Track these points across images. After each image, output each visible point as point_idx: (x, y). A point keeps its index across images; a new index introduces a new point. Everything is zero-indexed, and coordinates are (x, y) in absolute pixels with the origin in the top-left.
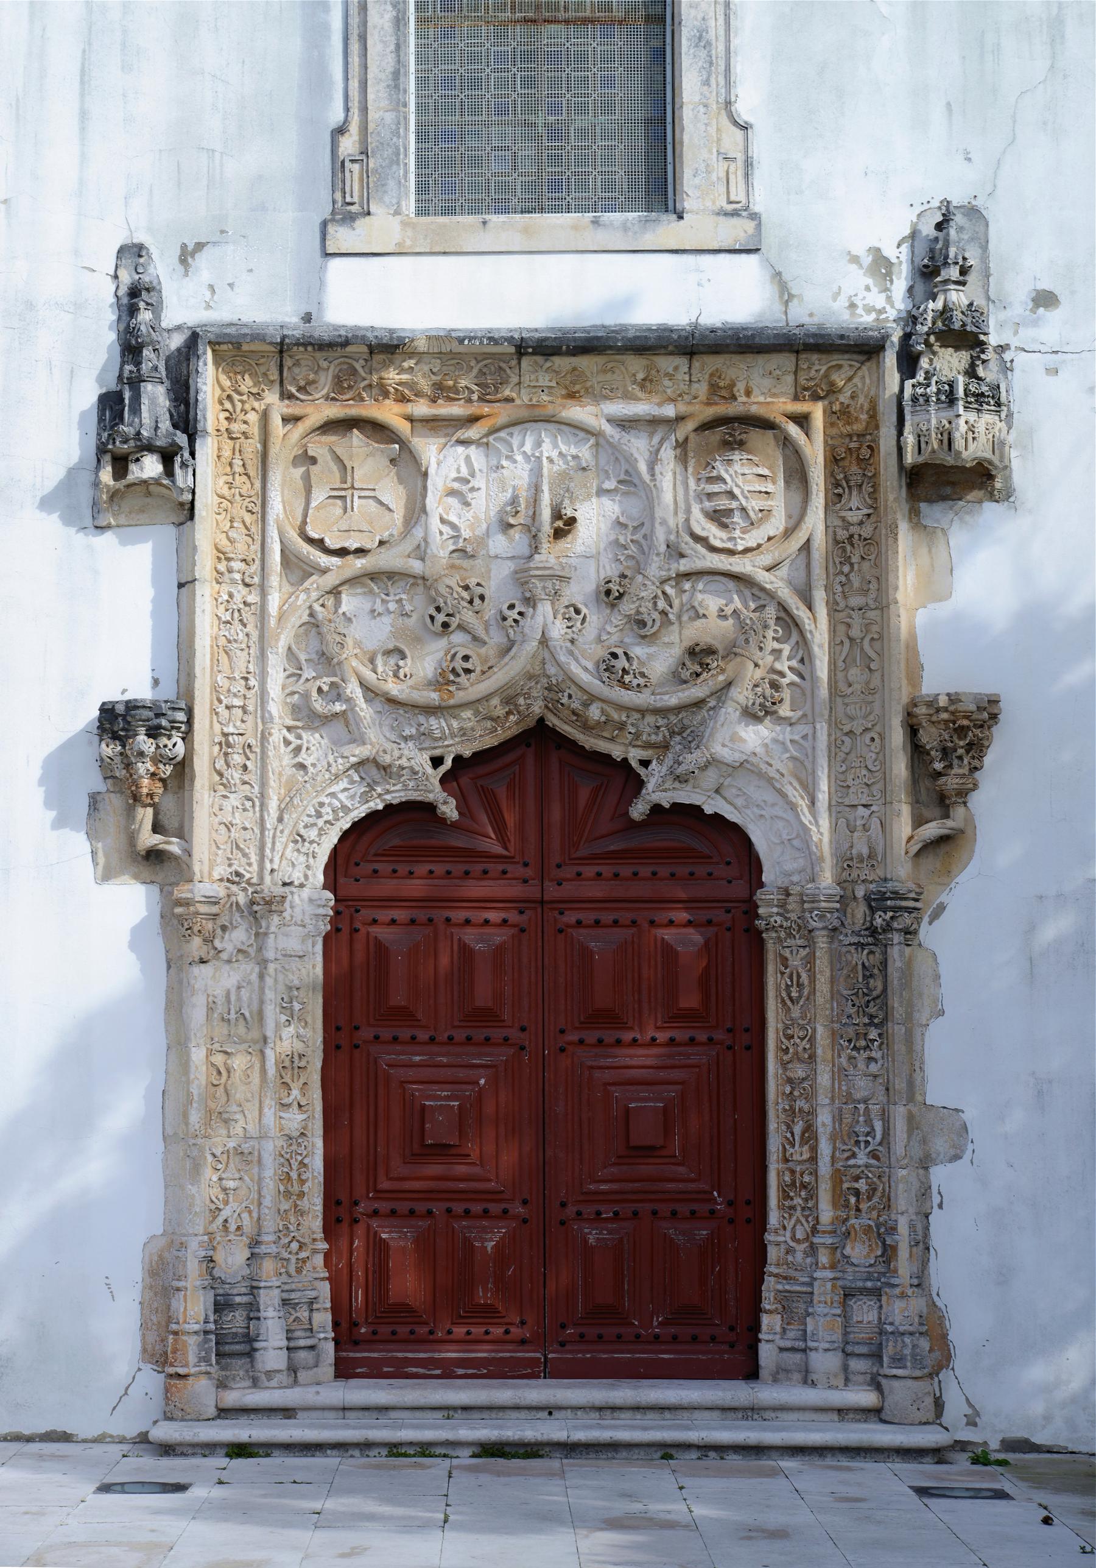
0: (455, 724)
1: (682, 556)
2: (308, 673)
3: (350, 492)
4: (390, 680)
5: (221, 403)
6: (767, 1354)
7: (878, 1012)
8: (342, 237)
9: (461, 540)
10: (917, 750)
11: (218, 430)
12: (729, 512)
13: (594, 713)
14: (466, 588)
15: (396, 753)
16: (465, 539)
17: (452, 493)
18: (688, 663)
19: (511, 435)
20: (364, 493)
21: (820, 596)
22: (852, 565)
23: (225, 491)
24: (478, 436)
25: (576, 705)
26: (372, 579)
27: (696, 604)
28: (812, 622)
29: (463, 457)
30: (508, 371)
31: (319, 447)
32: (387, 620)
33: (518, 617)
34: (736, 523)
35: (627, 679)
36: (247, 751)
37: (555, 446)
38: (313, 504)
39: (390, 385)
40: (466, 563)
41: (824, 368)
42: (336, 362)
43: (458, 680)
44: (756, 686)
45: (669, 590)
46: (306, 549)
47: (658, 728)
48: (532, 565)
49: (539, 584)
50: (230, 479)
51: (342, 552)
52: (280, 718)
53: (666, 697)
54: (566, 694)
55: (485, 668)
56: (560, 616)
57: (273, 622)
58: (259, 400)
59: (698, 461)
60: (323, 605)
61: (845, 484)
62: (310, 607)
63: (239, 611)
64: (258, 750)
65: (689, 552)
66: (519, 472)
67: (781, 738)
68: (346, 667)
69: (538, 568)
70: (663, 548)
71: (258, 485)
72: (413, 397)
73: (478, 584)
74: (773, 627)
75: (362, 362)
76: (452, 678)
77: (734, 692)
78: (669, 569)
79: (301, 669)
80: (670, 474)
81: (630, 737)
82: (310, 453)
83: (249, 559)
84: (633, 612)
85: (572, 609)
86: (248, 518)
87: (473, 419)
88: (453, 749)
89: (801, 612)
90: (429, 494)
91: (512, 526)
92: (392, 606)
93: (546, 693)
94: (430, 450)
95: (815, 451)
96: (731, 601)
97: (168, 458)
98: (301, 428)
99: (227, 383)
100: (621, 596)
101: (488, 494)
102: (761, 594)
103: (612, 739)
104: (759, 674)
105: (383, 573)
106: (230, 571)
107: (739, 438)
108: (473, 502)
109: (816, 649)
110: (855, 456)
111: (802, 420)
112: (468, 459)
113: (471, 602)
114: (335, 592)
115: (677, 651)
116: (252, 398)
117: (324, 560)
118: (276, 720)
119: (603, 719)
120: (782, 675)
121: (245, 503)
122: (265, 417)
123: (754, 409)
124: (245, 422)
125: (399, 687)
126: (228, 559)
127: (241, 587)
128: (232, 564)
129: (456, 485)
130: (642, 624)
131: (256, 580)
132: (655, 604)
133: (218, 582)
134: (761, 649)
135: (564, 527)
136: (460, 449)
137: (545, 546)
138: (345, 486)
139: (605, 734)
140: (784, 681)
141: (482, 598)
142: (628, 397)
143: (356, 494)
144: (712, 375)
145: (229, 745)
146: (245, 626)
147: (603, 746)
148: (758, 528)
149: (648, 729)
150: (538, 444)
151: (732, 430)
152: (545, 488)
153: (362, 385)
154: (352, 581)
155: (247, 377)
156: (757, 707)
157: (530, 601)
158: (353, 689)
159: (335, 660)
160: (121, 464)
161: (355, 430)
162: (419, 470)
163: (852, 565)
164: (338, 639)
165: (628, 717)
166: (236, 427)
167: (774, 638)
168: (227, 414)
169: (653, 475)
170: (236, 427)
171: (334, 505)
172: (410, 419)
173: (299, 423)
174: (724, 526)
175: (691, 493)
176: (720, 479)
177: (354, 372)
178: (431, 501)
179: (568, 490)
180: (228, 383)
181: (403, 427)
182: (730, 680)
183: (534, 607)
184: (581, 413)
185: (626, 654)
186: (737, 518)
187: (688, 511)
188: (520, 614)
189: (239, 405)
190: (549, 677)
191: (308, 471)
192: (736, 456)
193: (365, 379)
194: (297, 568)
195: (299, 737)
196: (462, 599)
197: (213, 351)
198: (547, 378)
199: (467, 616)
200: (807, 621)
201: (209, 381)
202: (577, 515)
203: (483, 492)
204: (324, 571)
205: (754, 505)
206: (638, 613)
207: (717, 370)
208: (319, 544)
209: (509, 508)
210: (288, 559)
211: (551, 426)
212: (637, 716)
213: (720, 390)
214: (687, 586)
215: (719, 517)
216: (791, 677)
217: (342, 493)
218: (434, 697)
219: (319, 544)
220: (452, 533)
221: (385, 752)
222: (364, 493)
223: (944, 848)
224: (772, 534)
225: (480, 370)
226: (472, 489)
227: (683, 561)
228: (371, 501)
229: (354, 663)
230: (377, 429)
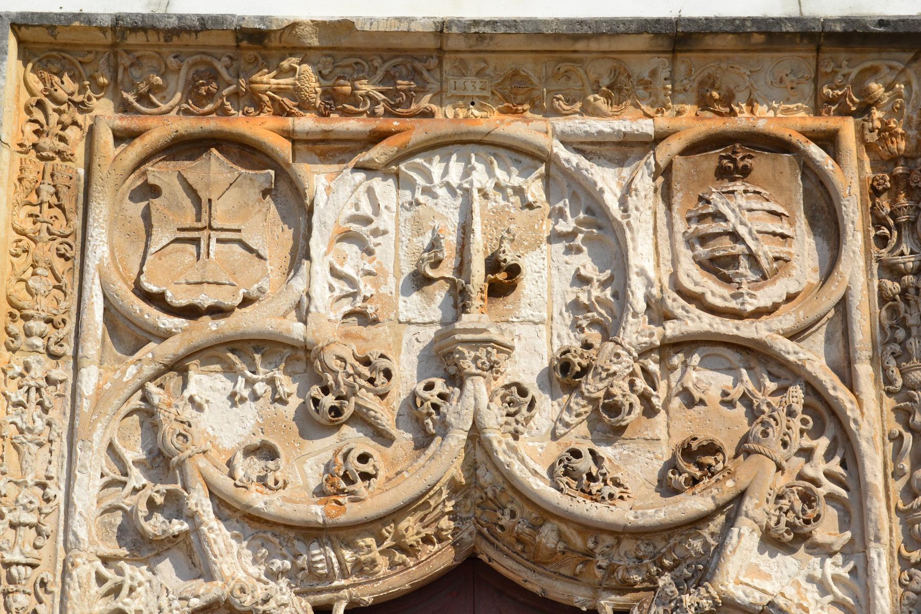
0: (348, 555)
1: (670, 316)
2: (137, 478)
3: (205, 233)
4: (253, 487)
5: (28, 111)
9: (359, 299)
11: (21, 145)
12: (733, 260)
13: (548, 537)
14: (367, 362)
15: (260, 594)
16: (365, 299)
17: (346, 237)
18: (682, 463)
19: (430, 161)
20: (224, 235)
21: (864, 371)
22: (908, 330)
23: (28, 226)
24: (383, 159)
25: (522, 528)
26: (233, 351)
27: (690, 385)
28: (856, 406)
29: (362, 189)
30: (426, 74)
31: (162, 173)
32: (249, 410)
33: (439, 401)
34: (742, 275)
35: (595, 487)
36: (40, 592)
37: (491, 173)
38: (152, 250)
39: (264, 92)
40: (367, 331)
41: (854, 72)
42: (191, 60)
43: (351, 488)
44: (780, 497)
45: (654, 367)
46: (139, 306)
47: (640, 559)
48: (458, 325)
49: (470, 354)
50: (36, 210)
51: (191, 312)
52: (92, 543)
53: (650, 512)
54: (507, 511)
55: (392, 473)
56: (497, 399)
57: (85, 405)
58: (82, 112)
59: (686, 195)
60: (161, 386)
61: (891, 222)
62: (142, 387)
63: (38, 390)
64: (57, 590)
65: (679, 312)
66: (441, 210)
67: (818, 574)
68: (189, 467)
69: (466, 331)
70: (641, 306)
71: (77, 222)
72: (296, 110)
73: (382, 356)
74: (800, 416)
75: (225, 59)
76: (343, 485)
77: (749, 504)
78: (652, 335)
79: (126, 474)
80: (649, 213)
81: (599, 573)
82: (152, 180)
83: (57, 319)
84: (601, 394)
85: (514, 389)
86: (60, 265)
87: (377, 137)
88: (345, 593)
89: (841, 394)
90: (315, 232)
91: (430, 281)
92: (260, 388)
93: (479, 512)
94: (318, 180)
95: (850, 178)
96: (738, 380)
98: (137, 148)
99: (38, 86)
100: (585, 371)
101: (398, 240)
102: (782, 372)
103: (574, 578)
104: (782, 481)
105: (249, 341)
106: (28, 334)
107: (741, 164)
108: (377, 250)
109: (864, 446)
110: (902, 184)
111: (829, 141)
112: (370, 191)
113: (371, 381)
114: (177, 368)
115: (665, 453)
116: (73, 108)
117: (166, 322)
118: (85, 545)
119: (561, 546)
120: (816, 482)
121: (55, 244)
122: (91, 135)
123: (761, 125)
124: (62, 139)
125: (266, 498)
126: (26, 318)
127: (44, 358)
128: (31, 323)
129: (354, 227)
130: (614, 409)
131: (68, 349)
132: (632, 384)
133: (9, 349)
134: (785, 445)
135: (504, 280)
136: (360, 176)
137: (477, 299)
138: (199, 225)
139: (563, 571)
140: (821, 492)
141: (388, 374)
142: (588, 110)
143: (214, 235)
144: (702, 83)
145: (11, 580)
146: (46, 411)
148: (774, 282)
149: (625, 562)
150: (467, 173)
151: (733, 155)
152: (477, 225)
153: (225, 92)
154: (206, 353)
155: (66, 78)
156: (783, 526)
157: (457, 379)
158: (199, 500)
159: (175, 459)
161: (214, 151)
162: (303, 205)
163: (908, 330)
164: (179, 428)
165: (596, 543)
166: (46, 142)
167: (802, 432)
168: (37, 126)
169: (625, 211)
170: (46, 142)
171: (184, 251)
172: (289, 135)
173: (137, 141)
174: (727, 280)
175: (679, 238)
176: (718, 216)
177: (214, 76)
178: (317, 244)
179: (508, 232)
180: (41, 86)
181: (284, 148)
182: (742, 486)
183: (461, 386)
184: (528, 129)
185: (592, 452)
186: (744, 266)
187: (675, 261)
188: (441, 396)
189: (54, 117)
190: (482, 488)
191: (148, 207)
192: (739, 186)
193: (229, 85)
194: (126, 334)
195: (120, 572)
196: (360, 375)
197: (20, 42)
198: (478, 85)
199: (369, 400)
200: (849, 406)
202: (521, 262)
203: (392, 235)
204: (163, 336)
205: (766, 250)
206: (609, 395)
207: (709, 76)
208: (157, 300)
209: (426, 255)
210: (112, 313)
211: (481, 150)
212: (609, 540)
214: (677, 360)
215: (718, 267)
216: (828, 487)
217: (195, 235)
218: (317, 512)
219: (157, 300)
220: (348, 289)
221: (243, 590)
222: (224, 235)
224: (792, 290)
225: (387, 72)
226: (376, 233)
227: (669, 325)
228: (236, 247)
229: (202, 462)
230: (246, 152)
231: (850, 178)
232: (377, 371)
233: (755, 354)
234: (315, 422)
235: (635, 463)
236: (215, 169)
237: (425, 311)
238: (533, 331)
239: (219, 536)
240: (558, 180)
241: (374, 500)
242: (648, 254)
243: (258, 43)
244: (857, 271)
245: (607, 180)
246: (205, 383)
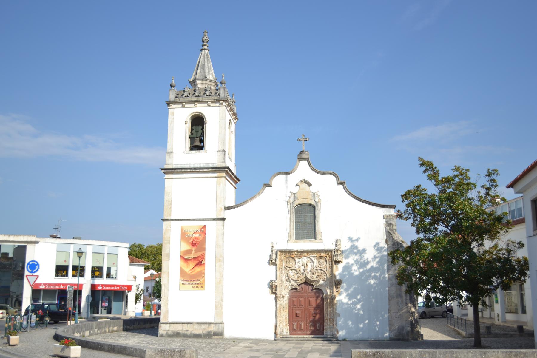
94: (296, 259)
95: (327, 259)
135: (307, 265)
151: (321, 257)
201: (279, 253)
215: (320, 264)
231: (327, 259)
232: (300, 271)
234: (297, 274)
235: (315, 276)
237: (302, 267)
238: (309, 269)
239: (291, 281)
240: (311, 259)
241: (300, 279)
242: (315, 264)
243: (293, 252)
244: (328, 265)
245: (313, 259)
246: (290, 271)
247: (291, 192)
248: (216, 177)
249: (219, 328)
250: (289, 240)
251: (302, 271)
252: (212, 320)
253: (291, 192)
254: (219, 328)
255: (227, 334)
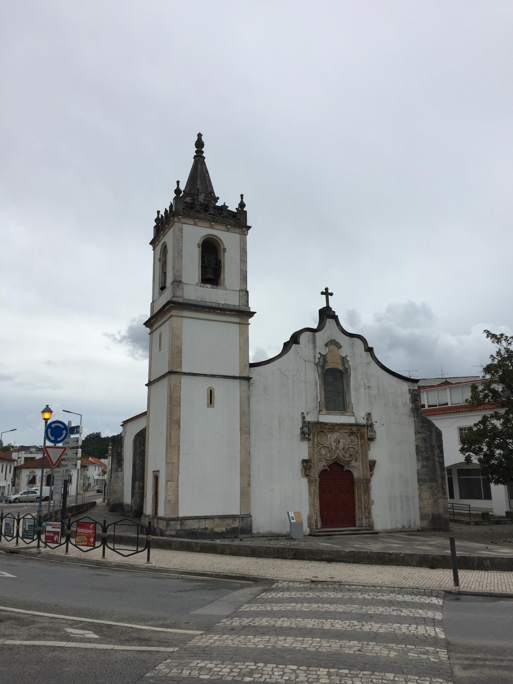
6: (357, 524)
7: (367, 490)
8: (321, 413)
10: (370, 465)
95: (359, 435)
97: (309, 435)
135: (339, 442)
147: (341, 464)
160: (304, 435)
213: (351, 430)
215: (351, 442)
223: (371, 475)
230: (323, 432)
231: (359, 435)
232: (332, 449)
233: (354, 448)
236: (322, 433)
238: (341, 445)
247: (319, 353)
248: (239, 323)
249: (247, 524)
250: (320, 411)
251: (334, 449)
252: (237, 512)
253: (319, 353)
254: (247, 524)
255: (254, 531)
